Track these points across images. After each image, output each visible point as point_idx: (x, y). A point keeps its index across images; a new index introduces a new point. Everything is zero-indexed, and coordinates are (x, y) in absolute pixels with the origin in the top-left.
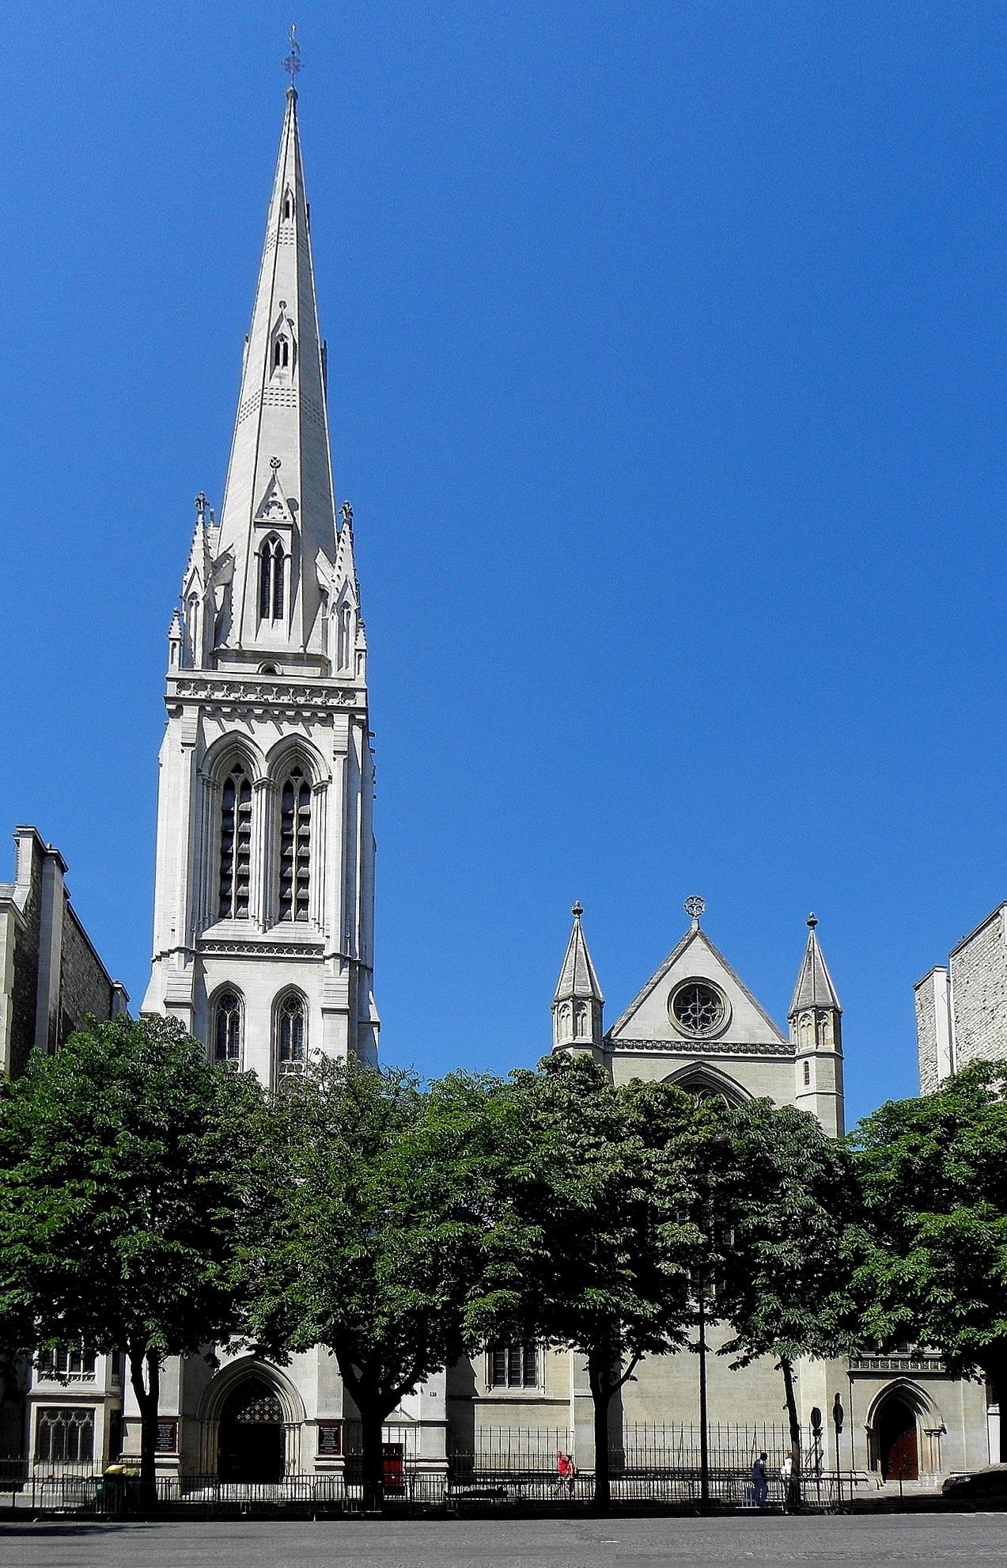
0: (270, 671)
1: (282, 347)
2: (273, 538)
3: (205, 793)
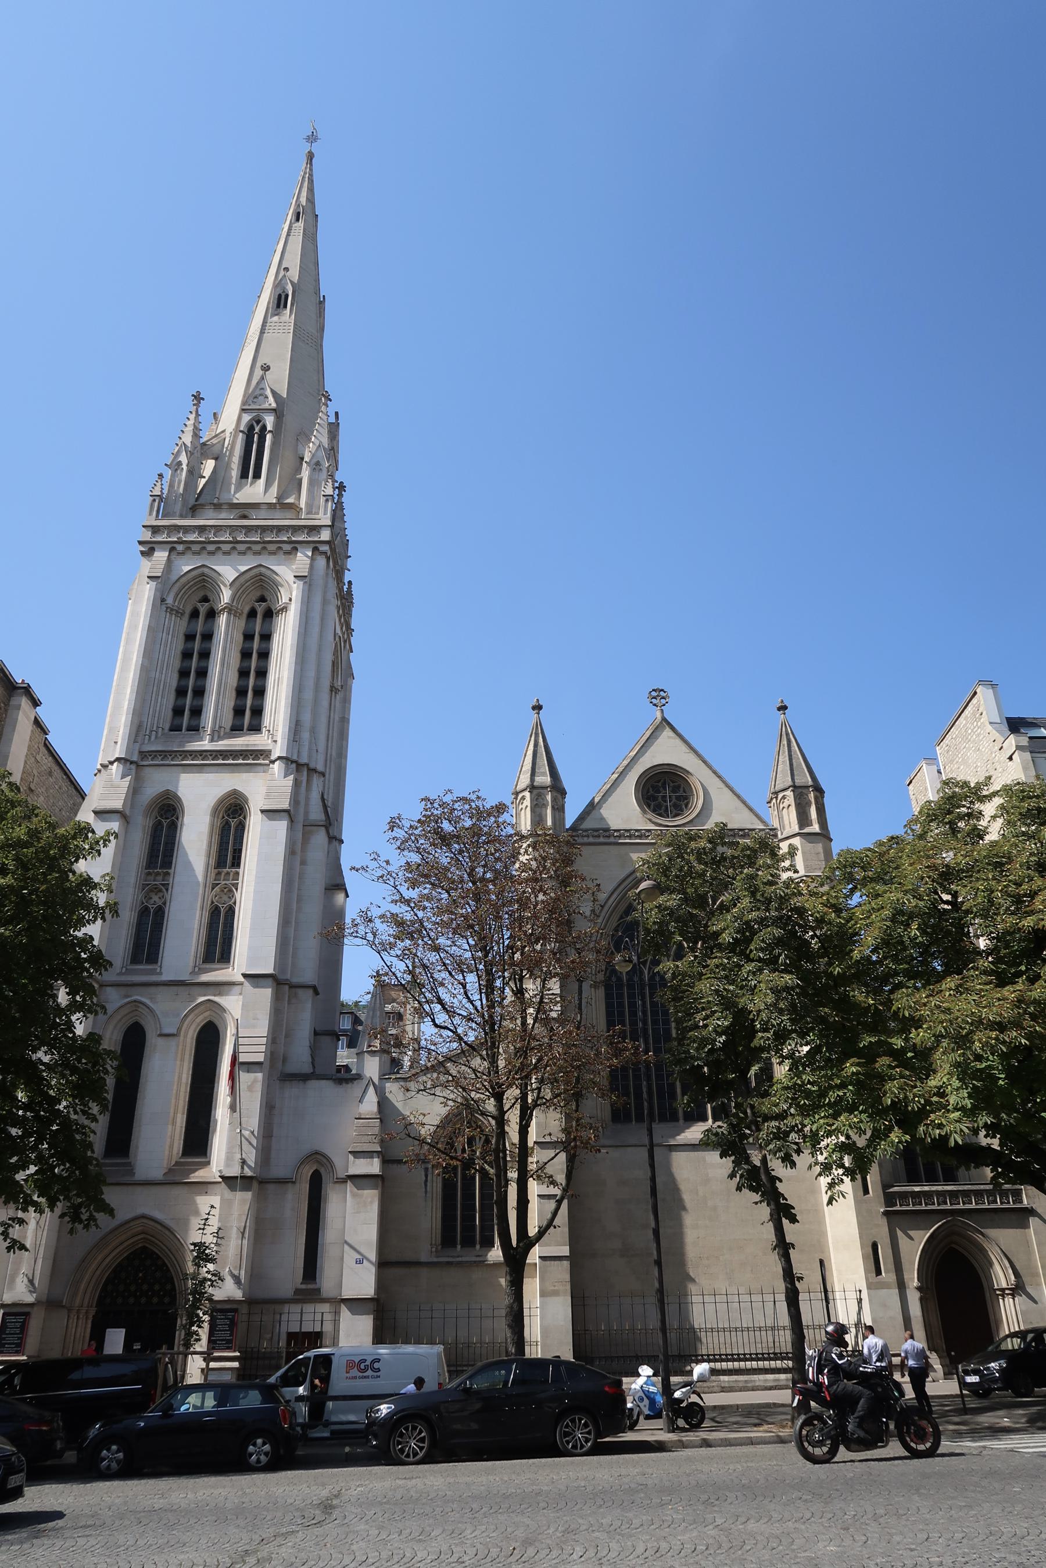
0: (245, 517)
1: (283, 297)
2: (258, 422)
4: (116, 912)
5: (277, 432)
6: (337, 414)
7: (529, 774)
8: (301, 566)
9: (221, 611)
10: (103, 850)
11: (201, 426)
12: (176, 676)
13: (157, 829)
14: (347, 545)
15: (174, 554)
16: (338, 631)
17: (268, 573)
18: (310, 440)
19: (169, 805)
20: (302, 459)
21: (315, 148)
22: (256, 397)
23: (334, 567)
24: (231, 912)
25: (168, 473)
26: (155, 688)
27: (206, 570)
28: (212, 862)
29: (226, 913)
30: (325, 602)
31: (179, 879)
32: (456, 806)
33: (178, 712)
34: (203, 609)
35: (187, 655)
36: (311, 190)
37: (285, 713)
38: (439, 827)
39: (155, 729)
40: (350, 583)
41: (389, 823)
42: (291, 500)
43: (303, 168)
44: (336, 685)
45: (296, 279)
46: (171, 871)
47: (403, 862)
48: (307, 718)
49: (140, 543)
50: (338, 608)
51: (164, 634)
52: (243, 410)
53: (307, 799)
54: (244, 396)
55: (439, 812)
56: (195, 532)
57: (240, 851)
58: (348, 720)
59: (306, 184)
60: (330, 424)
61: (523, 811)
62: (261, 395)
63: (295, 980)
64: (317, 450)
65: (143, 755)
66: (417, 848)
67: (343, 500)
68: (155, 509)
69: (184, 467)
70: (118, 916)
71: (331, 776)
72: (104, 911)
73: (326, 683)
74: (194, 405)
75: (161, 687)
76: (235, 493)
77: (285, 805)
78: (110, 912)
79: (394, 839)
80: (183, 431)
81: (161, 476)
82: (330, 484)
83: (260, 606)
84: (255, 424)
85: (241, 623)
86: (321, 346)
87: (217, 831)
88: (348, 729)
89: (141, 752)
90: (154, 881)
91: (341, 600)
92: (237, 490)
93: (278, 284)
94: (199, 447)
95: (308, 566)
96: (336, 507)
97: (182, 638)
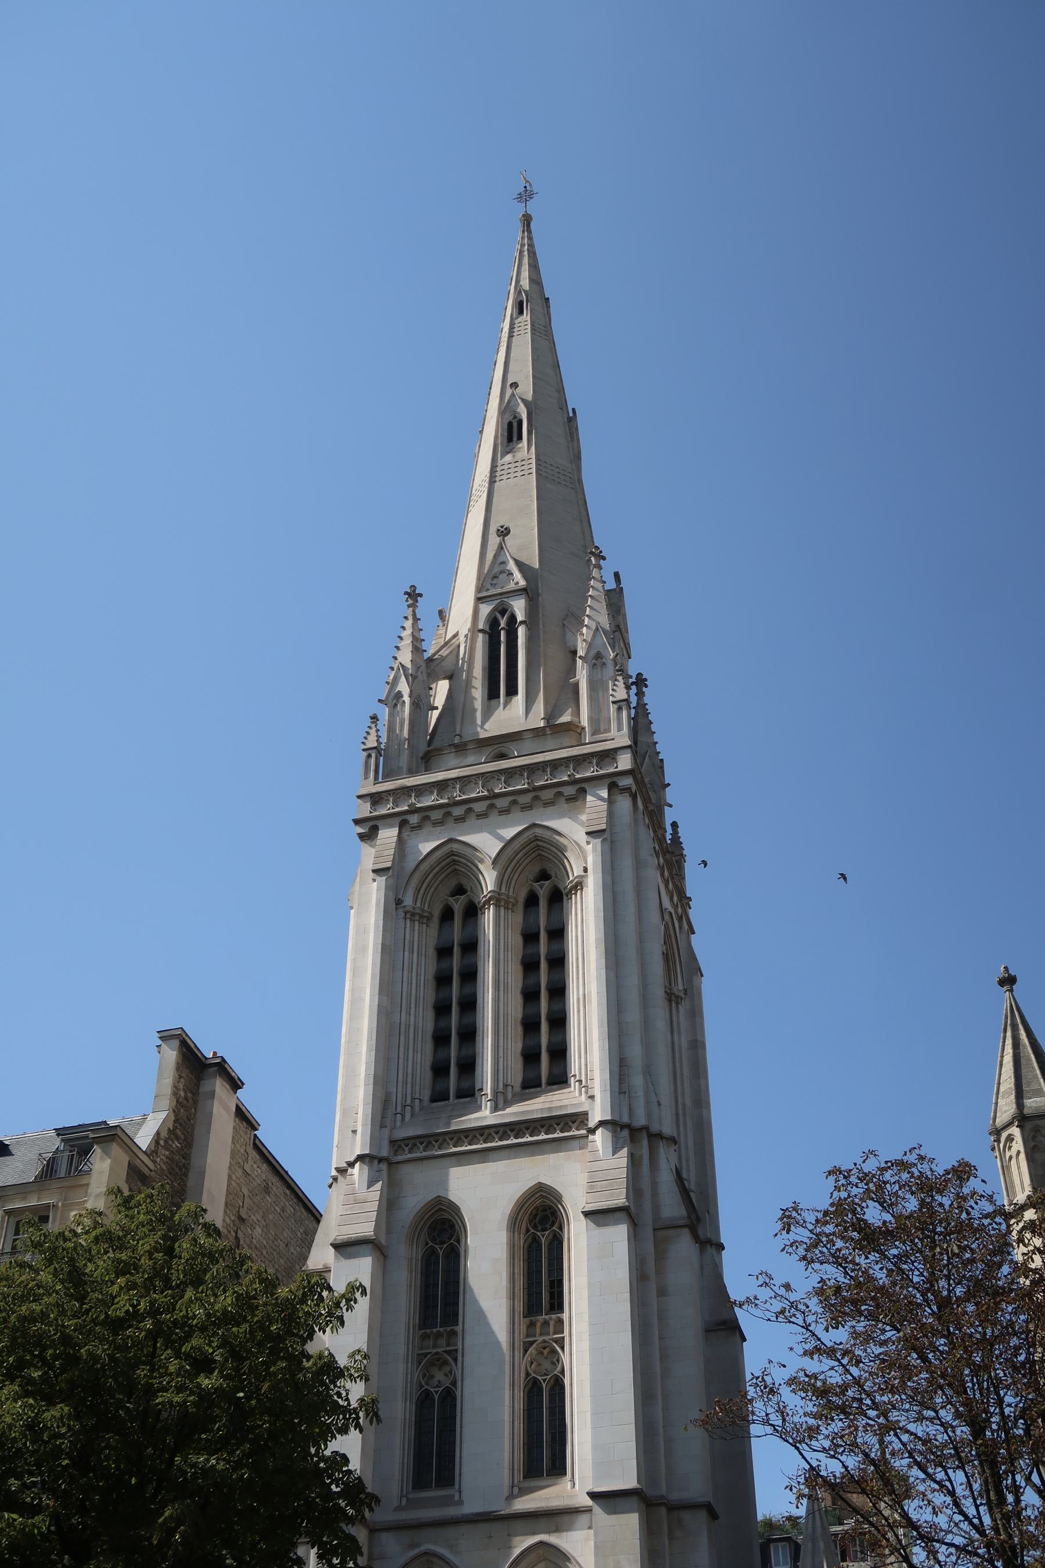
1: (515, 424)
2: (503, 612)
3: (408, 930)
4: (376, 1415)
5: (531, 622)
6: (617, 575)
7: (1013, 1097)
8: (595, 816)
9: (484, 904)
10: (347, 1316)
11: (422, 635)
12: (430, 1015)
13: (429, 1261)
14: (662, 768)
15: (407, 828)
16: (667, 904)
17: (547, 834)
18: (582, 624)
19: (444, 1221)
20: (575, 653)
21: (532, 207)
22: (495, 577)
23: (646, 807)
24: (558, 1388)
25: (384, 712)
26: (402, 1038)
27: (455, 846)
28: (520, 1307)
29: (552, 1389)
30: (639, 865)
31: (471, 1341)
32: (887, 1176)
33: (440, 1070)
34: (458, 906)
35: (442, 980)
36: (534, 266)
37: (601, 1050)
38: (859, 1220)
39: (409, 1102)
40: (674, 825)
41: (781, 1219)
42: (566, 718)
43: (519, 239)
44: (675, 991)
45: (529, 396)
46: (459, 1328)
47: (814, 1282)
48: (635, 1052)
49: (357, 822)
50: (661, 868)
51: (406, 953)
52: (479, 600)
53: (654, 1184)
54: (478, 578)
55: (861, 1191)
56: (432, 793)
57: (560, 1282)
58: (703, 1043)
59: (526, 260)
60: (608, 593)
61: (1014, 1161)
62: (502, 572)
63: (675, 1496)
64: (594, 636)
65: (396, 1145)
66: (833, 1256)
67: (646, 700)
68: (373, 768)
69: (406, 698)
70: (379, 1421)
71: (688, 1140)
72: (357, 1414)
73: (658, 992)
74: (409, 606)
75: (411, 1035)
76: (483, 722)
77: (620, 1199)
78: (367, 1415)
79: (791, 1246)
80: (398, 648)
81: (374, 718)
82: (621, 683)
83: (541, 887)
84: (499, 616)
85: (517, 918)
86: (580, 481)
87: (520, 1255)
88: (705, 1059)
89: (393, 1142)
90: (435, 1346)
91: (664, 856)
92: (485, 719)
93: (507, 408)
94: (424, 665)
95: (605, 814)
96: (636, 713)
97: (432, 953)
